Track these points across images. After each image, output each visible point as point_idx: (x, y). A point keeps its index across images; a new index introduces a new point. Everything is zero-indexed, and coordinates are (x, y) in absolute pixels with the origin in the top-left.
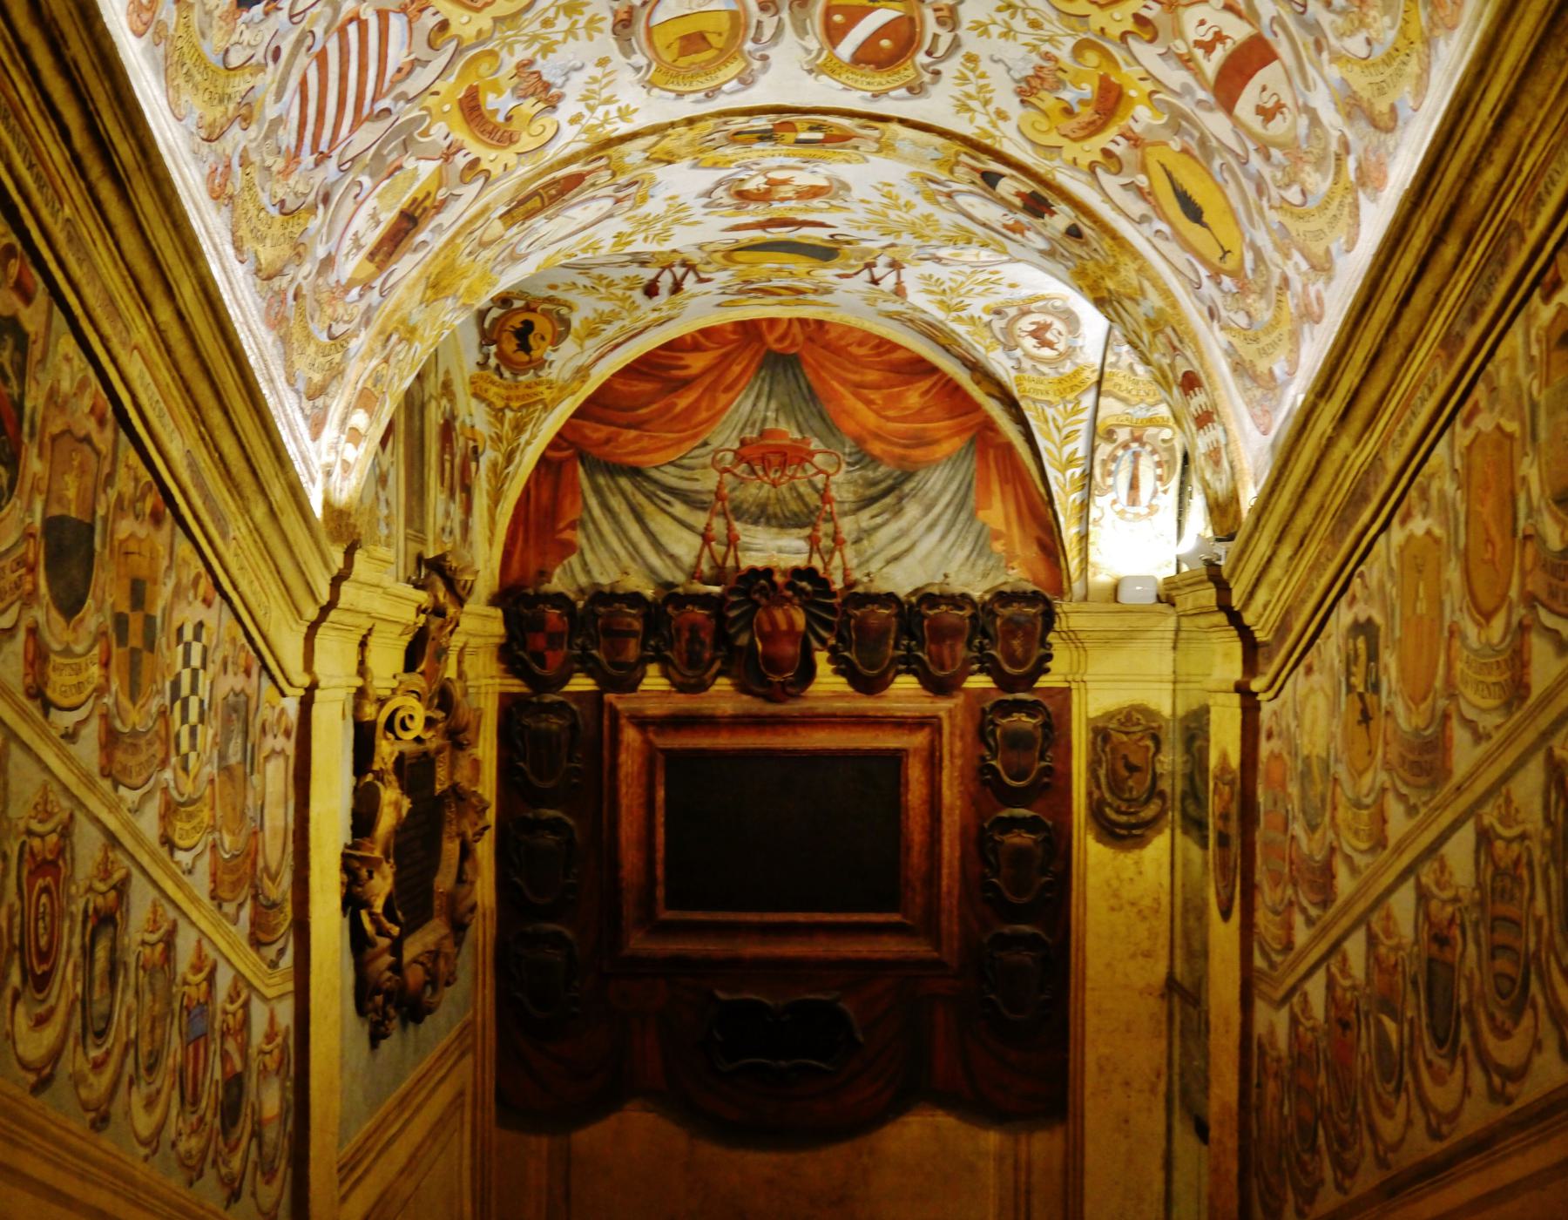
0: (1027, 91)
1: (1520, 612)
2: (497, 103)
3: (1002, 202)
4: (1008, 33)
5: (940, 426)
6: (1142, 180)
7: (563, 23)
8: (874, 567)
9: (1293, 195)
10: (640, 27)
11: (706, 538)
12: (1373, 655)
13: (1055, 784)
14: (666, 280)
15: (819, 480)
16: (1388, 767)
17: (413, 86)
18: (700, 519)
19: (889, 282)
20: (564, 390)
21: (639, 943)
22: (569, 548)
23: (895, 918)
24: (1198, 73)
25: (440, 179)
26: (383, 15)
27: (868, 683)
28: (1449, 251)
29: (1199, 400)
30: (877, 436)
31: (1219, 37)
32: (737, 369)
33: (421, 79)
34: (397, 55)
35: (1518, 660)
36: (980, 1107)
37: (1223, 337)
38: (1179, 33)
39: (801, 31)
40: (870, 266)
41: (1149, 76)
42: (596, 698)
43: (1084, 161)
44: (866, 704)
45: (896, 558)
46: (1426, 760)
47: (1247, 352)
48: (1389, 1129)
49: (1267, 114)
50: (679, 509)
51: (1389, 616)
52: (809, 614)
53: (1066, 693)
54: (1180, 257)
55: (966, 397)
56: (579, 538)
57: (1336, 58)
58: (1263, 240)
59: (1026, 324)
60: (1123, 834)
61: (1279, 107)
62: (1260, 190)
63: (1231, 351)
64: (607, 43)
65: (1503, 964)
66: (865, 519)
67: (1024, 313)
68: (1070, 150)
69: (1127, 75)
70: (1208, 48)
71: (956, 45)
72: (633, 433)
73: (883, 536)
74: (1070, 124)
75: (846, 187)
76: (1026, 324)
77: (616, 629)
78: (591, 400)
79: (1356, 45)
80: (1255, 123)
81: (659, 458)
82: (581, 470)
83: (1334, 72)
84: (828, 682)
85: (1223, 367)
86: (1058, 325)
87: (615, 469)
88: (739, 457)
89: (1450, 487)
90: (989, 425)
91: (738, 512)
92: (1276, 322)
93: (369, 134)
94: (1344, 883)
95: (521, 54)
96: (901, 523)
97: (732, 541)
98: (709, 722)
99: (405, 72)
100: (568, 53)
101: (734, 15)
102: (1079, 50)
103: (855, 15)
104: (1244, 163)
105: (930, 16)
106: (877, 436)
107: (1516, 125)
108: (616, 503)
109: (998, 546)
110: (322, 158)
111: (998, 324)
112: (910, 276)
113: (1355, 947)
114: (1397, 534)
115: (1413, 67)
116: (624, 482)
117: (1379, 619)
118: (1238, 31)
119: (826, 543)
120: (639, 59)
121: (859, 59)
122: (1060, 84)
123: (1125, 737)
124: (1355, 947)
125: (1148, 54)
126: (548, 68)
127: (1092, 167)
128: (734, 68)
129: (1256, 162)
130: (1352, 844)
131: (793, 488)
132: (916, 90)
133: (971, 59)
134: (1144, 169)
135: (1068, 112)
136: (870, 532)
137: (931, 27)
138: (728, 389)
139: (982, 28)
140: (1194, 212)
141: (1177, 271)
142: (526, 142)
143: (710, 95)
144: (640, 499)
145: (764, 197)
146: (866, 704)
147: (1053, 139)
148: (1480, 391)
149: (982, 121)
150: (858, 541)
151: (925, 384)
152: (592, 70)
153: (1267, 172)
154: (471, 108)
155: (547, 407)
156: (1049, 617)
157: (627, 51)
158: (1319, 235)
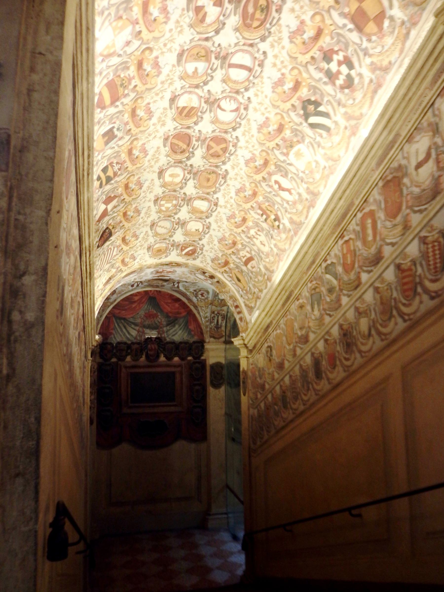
0: (213, 260)
1: (295, 344)
2: (127, 260)
3: (206, 276)
4: (211, 252)
5: (182, 310)
6: (231, 275)
7: (140, 248)
8: (170, 337)
9: (256, 280)
10: (151, 249)
11: (138, 331)
12: (271, 350)
13: (204, 376)
14: (136, 285)
15: (160, 320)
16: (274, 367)
17: (115, 258)
18: (137, 328)
19: (176, 286)
20: (112, 303)
21: (126, 410)
22: (111, 334)
23: (175, 403)
24: (242, 260)
25: (116, 272)
26: (114, 248)
27: (169, 358)
28: (283, 292)
29: (238, 310)
30: (171, 313)
31: (245, 256)
32: (144, 300)
33: (117, 256)
34: (115, 253)
35: (295, 351)
36: (192, 439)
37: (243, 300)
38: (239, 254)
39: (177, 250)
40: (174, 283)
41: (233, 260)
42: (116, 363)
43: (221, 271)
44: (169, 362)
45: (174, 335)
46: (281, 366)
47: (247, 303)
48: (276, 423)
49: (253, 268)
50: (133, 326)
51: (274, 345)
52: (159, 346)
53: (205, 360)
54: (236, 287)
55: (187, 305)
56: (114, 332)
57: (264, 261)
58: (251, 286)
59: (200, 293)
60: (216, 386)
61: (254, 267)
62: (251, 278)
63: (244, 302)
64: (146, 251)
65: (294, 394)
66: (168, 328)
67: (200, 291)
68: (219, 270)
69: (230, 260)
70: (244, 257)
71: (202, 253)
72: (124, 312)
73: (171, 331)
74: (219, 266)
75: (176, 271)
76: (200, 293)
77: (126, 348)
78: (116, 305)
79: (267, 260)
80: (250, 268)
81: (129, 316)
82: (114, 319)
83: (264, 263)
84: (162, 358)
85: (243, 305)
86: (206, 293)
87: (120, 319)
88: (145, 316)
89: (283, 326)
90: (191, 310)
91: (144, 327)
92: (253, 298)
93: (109, 265)
94: (267, 386)
95: (132, 252)
96: (174, 329)
97: (143, 333)
98: (140, 367)
99: (115, 256)
100: (139, 252)
101: (166, 247)
102: (222, 256)
103: (186, 248)
104: (248, 274)
105: (198, 249)
106: (171, 313)
107: (293, 278)
108: (121, 325)
109: (193, 333)
110: (101, 270)
111: (195, 293)
112: (180, 285)
113: (270, 396)
114: (275, 333)
115: (276, 265)
116: (122, 321)
117: (272, 345)
118: (248, 255)
119: (161, 332)
120: (150, 253)
121: (186, 254)
122: (219, 260)
123: (217, 367)
124: (270, 396)
125: (234, 257)
126: (136, 255)
127: (222, 272)
128: (165, 255)
129: (250, 274)
130: (268, 380)
131: (155, 322)
132: (194, 259)
133: (204, 255)
134: (231, 273)
135: (219, 264)
136: (169, 330)
137: (198, 250)
138: (143, 303)
139: (207, 251)
140: (239, 280)
141: (236, 289)
142: (129, 266)
143: (160, 259)
144: (126, 324)
145: (161, 272)
146: (169, 362)
147: (216, 268)
148: (288, 313)
149: (205, 264)
150: (167, 332)
151: (179, 303)
152: (142, 255)
153: (252, 276)
154: (123, 261)
155: (109, 306)
156: (203, 346)
157: (148, 252)
158: (260, 286)
